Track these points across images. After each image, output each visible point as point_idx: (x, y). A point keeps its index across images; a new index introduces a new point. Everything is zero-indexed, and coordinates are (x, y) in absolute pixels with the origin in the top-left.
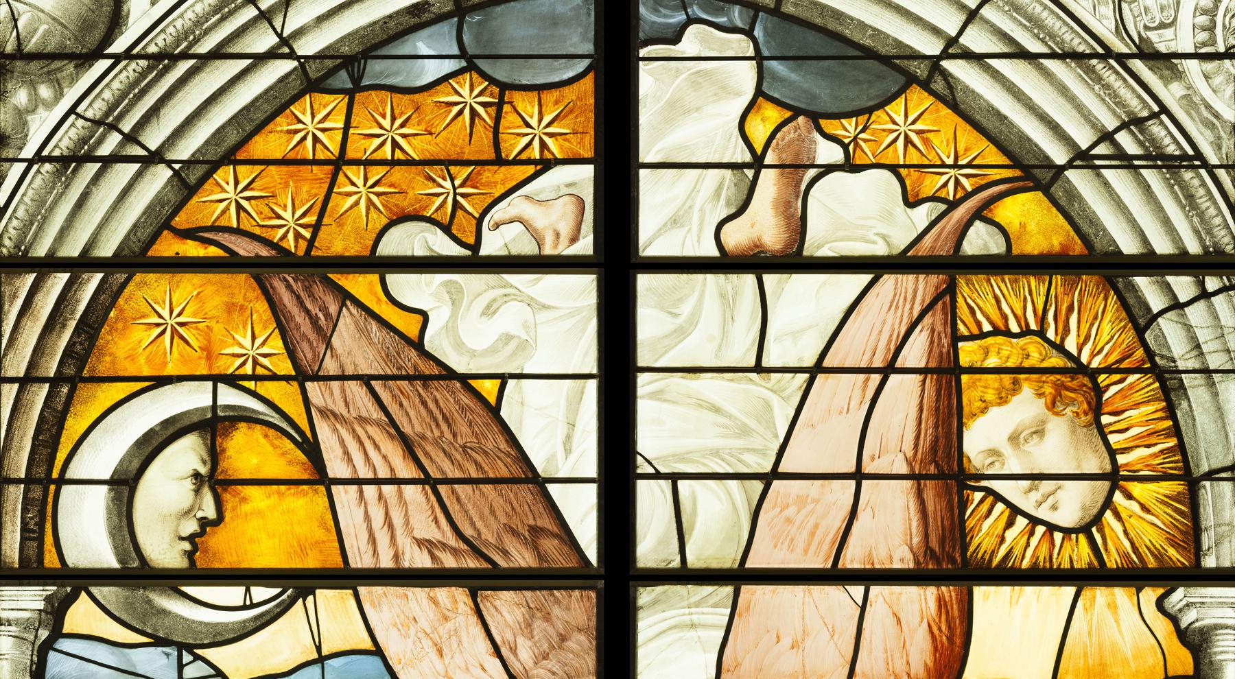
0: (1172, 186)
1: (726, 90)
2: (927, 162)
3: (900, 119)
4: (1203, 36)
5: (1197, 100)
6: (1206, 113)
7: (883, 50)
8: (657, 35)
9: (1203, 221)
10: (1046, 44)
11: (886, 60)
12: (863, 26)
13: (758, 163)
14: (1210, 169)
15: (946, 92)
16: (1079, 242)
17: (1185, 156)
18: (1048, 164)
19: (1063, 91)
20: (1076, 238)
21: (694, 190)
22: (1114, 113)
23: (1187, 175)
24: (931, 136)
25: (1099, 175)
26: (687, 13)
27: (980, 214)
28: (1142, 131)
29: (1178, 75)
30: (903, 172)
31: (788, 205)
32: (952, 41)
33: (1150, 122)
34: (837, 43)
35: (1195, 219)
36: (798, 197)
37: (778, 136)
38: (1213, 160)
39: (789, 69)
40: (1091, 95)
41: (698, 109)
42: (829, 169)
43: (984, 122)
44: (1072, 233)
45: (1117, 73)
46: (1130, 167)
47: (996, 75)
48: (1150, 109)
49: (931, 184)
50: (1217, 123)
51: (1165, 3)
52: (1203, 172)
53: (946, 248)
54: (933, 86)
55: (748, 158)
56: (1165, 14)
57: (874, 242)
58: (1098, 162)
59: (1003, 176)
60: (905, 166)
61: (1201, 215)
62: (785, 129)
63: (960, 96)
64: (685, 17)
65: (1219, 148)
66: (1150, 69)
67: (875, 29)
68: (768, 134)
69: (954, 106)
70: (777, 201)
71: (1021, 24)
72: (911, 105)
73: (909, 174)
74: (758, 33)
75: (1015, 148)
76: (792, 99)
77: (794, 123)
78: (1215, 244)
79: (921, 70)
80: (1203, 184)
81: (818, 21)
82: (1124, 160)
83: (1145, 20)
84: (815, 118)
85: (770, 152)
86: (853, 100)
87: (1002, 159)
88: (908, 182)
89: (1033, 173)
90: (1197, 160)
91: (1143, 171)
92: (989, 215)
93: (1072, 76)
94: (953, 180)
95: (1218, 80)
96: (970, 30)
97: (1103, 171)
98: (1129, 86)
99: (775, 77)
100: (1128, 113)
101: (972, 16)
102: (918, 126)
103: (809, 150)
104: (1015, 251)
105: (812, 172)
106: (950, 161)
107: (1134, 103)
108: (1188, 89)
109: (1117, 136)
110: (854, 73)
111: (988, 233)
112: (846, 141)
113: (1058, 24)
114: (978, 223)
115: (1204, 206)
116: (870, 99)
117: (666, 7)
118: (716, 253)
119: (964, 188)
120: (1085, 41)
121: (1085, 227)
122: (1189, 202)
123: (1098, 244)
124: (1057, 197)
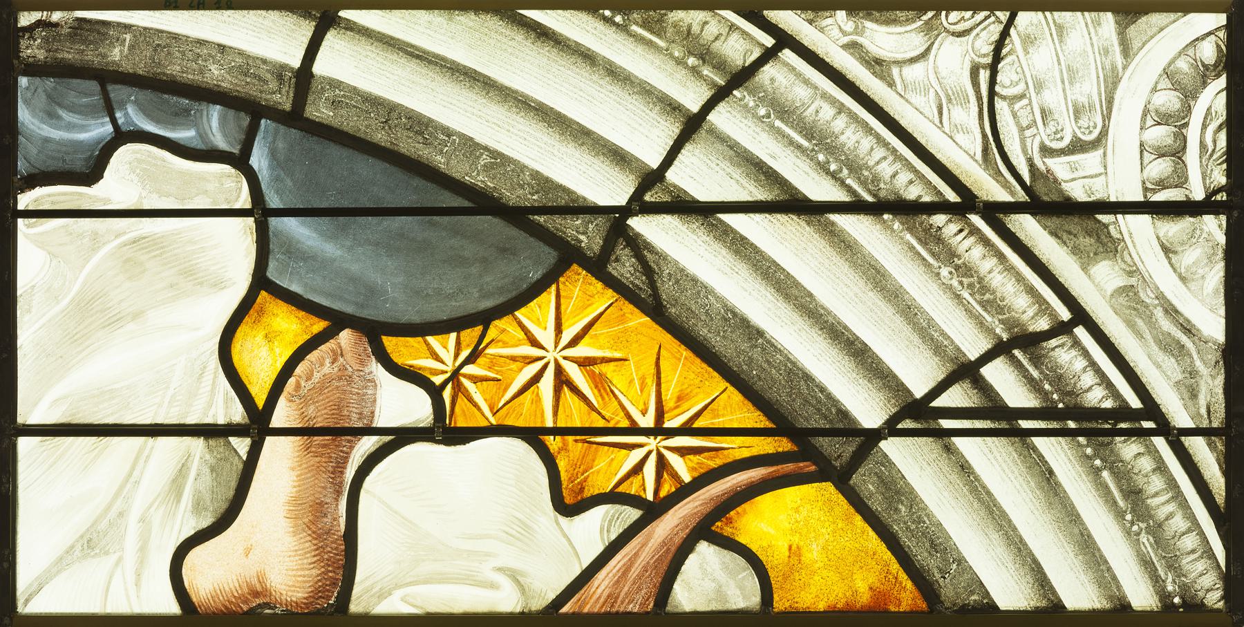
0: (1096, 472)
1: (193, 278)
2: (600, 423)
3: (546, 336)
4: (1162, 168)
5: (1147, 296)
6: (1166, 325)
7: (512, 196)
8: (53, 165)
9: (1159, 543)
10: (842, 183)
11: (518, 216)
12: (470, 146)
13: (258, 425)
14: (1175, 437)
15: (640, 281)
16: (909, 585)
17: (1123, 412)
18: (846, 428)
19: (877, 278)
20: (903, 576)
21: (130, 480)
22: (981, 324)
23: (1128, 449)
24: (608, 369)
25: (949, 449)
26: (114, 121)
27: (705, 529)
28: (1036, 361)
29: (1109, 246)
30: (553, 442)
31: (319, 509)
32: (652, 178)
33: (1053, 342)
34: (417, 182)
35: (1144, 538)
36: (339, 493)
37: (300, 369)
38: (1181, 418)
39: (322, 234)
40: (934, 287)
41: (136, 316)
42: (403, 436)
43: (716, 343)
44: (895, 566)
45: (986, 242)
46: (1014, 433)
47: (741, 247)
48: (1053, 314)
49: (609, 467)
50: (1189, 344)
51: (1083, 100)
52: (1160, 442)
53: (639, 598)
54: (613, 269)
55: (237, 414)
56: (1084, 122)
57: (493, 586)
58: (946, 424)
59: (755, 451)
60: (556, 431)
61: (1156, 530)
62: (313, 356)
63: (667, 289)
64: (109, 128)
65: (1194, 394)
66: (1054, 234)
67: (495, 154)
68: (279, 365)
69: (656, 310)
70: (296, 501)
71: (791, 142)
72: (568, 308)
73: (564, 448)
74: (258, 160)
75: (779, 395)
76: (328, 295)
77: (331, 344)
78: (1185, 590)
79: (588, 236)
80: (1161, 468)
81: (380, 137)
82: (1000, 420)
83: (1044, 134)
84: (374, 333)
85: (282, 403)
86: (450, 297)
87: (753, 418)
88: (562, 464)
89: (816, 447)
90: (1147, 418)
91: (1038, 441)
92: (727, 531)
93: (896, 248)
94: (652, 460)
95: (1190, 257)
96: (688, 154)
97: (958, 441)
98: (1010, 269)
99: (293, 251)
100: (1009, 324)
101: (692, 126)
102: (582, 350)
103: (362, 397)
104: (780, 604)
105: (368, 444)
106: (648, 421)
107: (1021, 305)
108: (1130, 274)
109: (988, 371)
110: (455, 242)
111: (725, 567)
112: (438, 380)
113: (867, 142)
114: (703, 547)
115: (1162, 513)
116: (485, 296)
117: (72, 109)
118: (173, 608)
119: (675, 476)
120: (922, 177)
121: (921, 555)
122: (1132, 503)
123: (949, 591)
124: (864, 494)
